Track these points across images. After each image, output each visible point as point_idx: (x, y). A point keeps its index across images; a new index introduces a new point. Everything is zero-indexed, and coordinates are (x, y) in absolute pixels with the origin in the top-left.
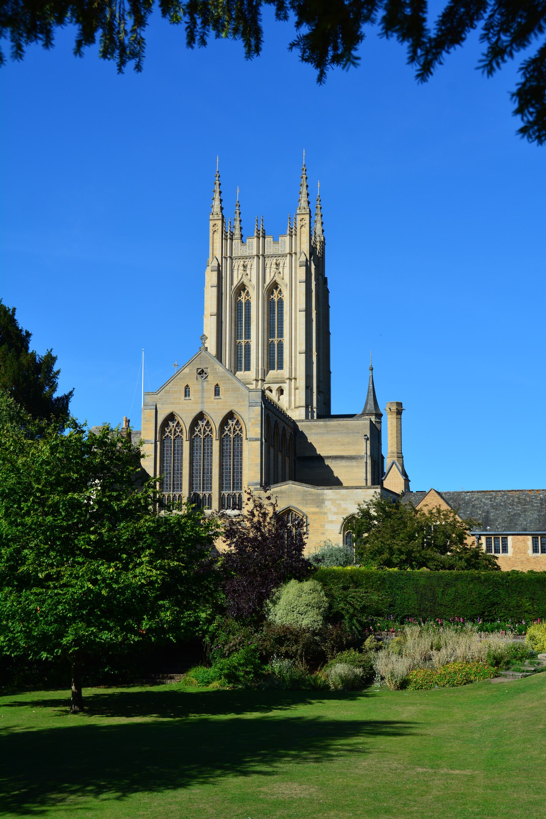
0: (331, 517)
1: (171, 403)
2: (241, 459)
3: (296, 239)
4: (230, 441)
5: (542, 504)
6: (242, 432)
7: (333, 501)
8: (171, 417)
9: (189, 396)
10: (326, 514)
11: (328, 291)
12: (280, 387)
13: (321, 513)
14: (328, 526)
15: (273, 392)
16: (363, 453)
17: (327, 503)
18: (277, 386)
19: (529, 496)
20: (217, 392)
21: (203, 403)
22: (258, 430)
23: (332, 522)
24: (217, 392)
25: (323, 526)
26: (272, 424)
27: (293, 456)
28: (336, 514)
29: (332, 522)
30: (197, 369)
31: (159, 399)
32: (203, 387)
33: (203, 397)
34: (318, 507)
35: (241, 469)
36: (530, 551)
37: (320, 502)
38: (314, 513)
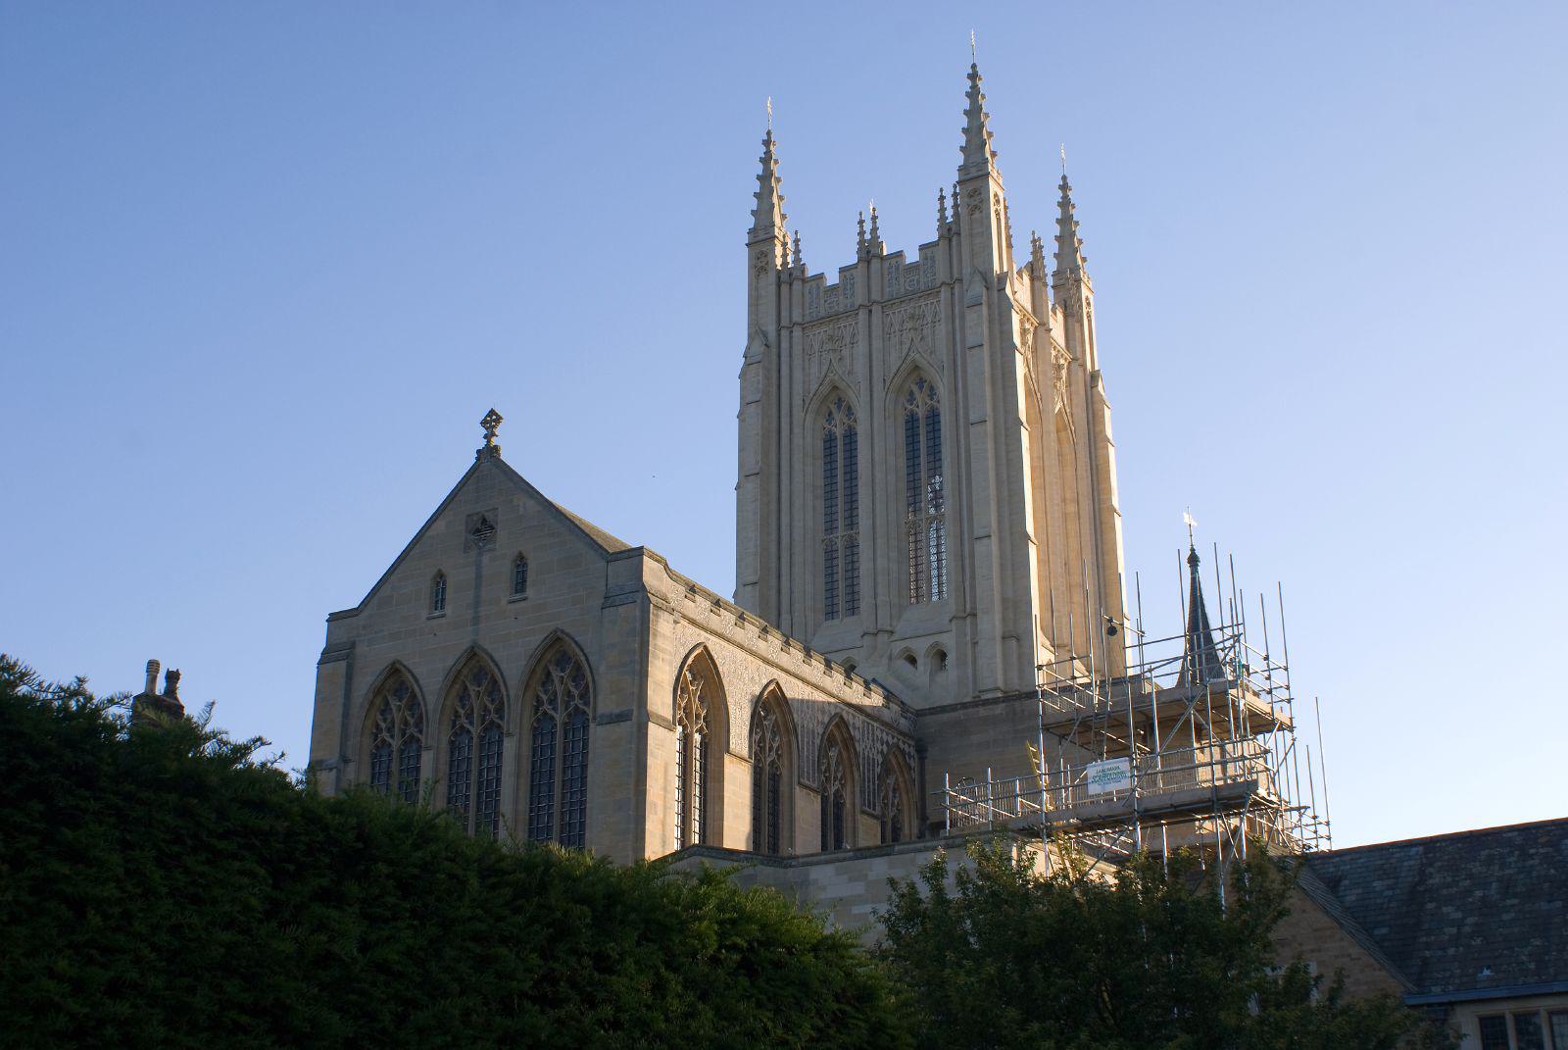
2: (583, 793)
3: (959, 244)
4: (553, 734)
6: (587, 704)
9: (442, 608)
12: (937, 643)
15: (920, 661)
18: (931, 640)
20: (520, 584)
21: (476, 620)
24: (520, 584)
27: (915, 823)
30: (469, 516)
31: (364, 627)
32: (479, 567)
33: (477, 603)
35: (582, 825)
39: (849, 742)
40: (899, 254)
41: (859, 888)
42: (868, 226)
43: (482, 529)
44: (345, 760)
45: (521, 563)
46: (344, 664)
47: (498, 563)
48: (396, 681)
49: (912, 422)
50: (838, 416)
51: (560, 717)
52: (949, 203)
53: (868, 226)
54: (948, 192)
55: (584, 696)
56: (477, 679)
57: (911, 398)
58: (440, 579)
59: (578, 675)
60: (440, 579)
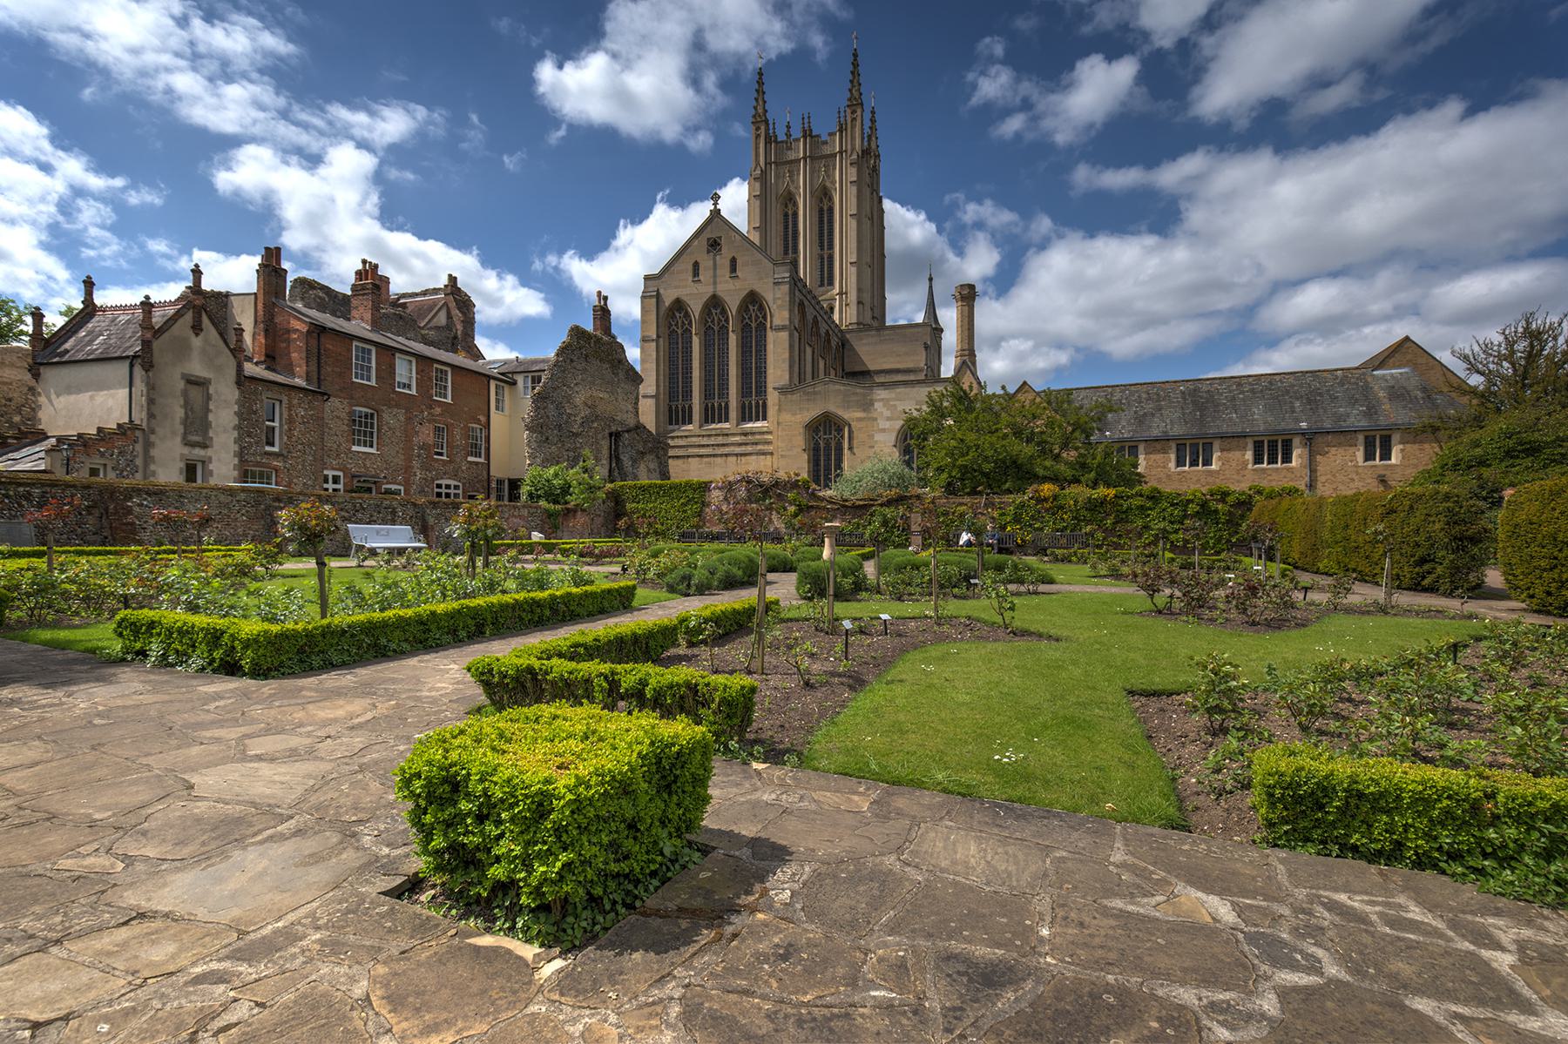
0: (882, 424)
1: (676, 287)
5: (1185, 399)
7: (885, 401)
8: (679, 305)
10: (876, 419)
11: (883, 211)
13: (869, 419)
14: (878, 437)
16: (922, 364)
17: (877, 405)
19: (1163, 390)
21: (715, 283)
22: (786, 314)
23: (883, 430)
25: (871, 437)
26: (810, 318)
28: (888, 419)
29: (883, 430)
33: (715, 276)
34: (864, 410)
36: (1172, 465)
37: (867, 406)
38: (860, 420)
39: (829, 341)
40: (818, 136)
41: (893, 396)
42: (806, 121)
43: (714, 245)
44: (658, 336)
45: (733, 261)
46: (654, 300)
47: (723, 261)
48: (679, 305)
49: (821, 211)
50: (790, 206)
51: (753, 325)
52: (842, 114)
53: (806, 121)
54: (842, 110)
55: (765, 317)
56: (715, 307)
57: (821, 201)
58: (696, 265)
59: (761, 308)
60: (696, 265)
